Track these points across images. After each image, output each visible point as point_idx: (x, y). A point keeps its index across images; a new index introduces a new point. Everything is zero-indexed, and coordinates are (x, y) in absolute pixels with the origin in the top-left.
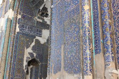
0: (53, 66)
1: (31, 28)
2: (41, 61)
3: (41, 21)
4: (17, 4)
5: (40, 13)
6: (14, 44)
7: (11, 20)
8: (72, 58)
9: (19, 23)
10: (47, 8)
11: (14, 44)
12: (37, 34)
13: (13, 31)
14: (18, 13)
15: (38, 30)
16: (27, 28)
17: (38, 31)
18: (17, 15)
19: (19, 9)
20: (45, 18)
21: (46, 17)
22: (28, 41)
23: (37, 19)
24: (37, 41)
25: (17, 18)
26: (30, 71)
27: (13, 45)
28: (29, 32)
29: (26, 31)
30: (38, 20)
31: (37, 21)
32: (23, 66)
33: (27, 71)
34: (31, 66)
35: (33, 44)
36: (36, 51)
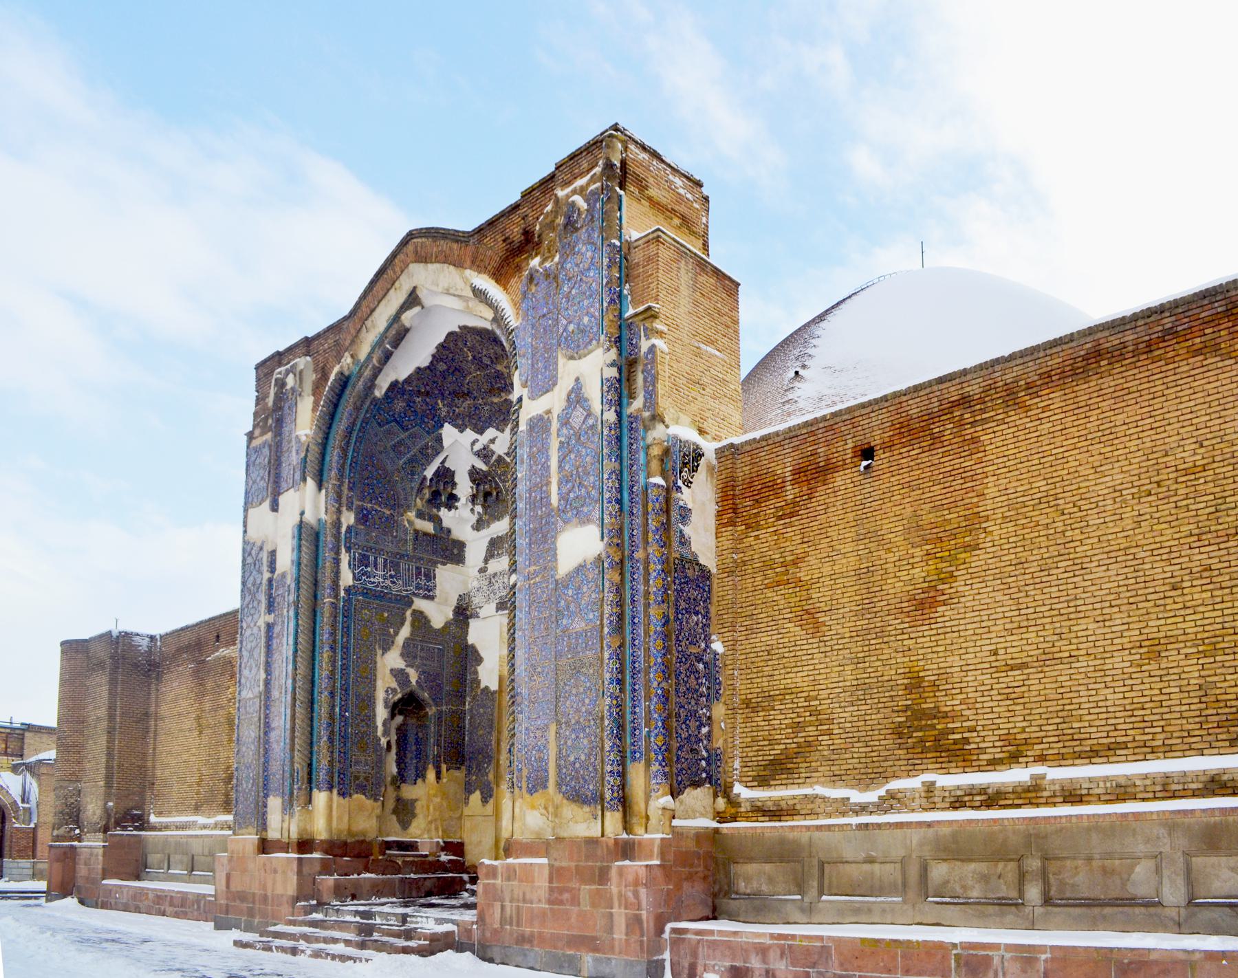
0: (525, 772)
1: (396, 566)
2: (437, 701)
5: (427, 494)
6: (339, 637)
7: (317, 535)
8: (577, 765)
9: (348, 550)
11: (339, 637)
12: (418, 587)
13: (328, 583)
16: (380, 566)
17: (420, 573)
18: (339, 512)
22: (387, 623)
24: (421, 620)
26: (394, 738)
27: (334, 641)
29: (378, 578)
31: (416, 532)
32: (375, 723)
33: (389, 743)
34: (399, 719)
35: (405, 632)
36: (418, 661)
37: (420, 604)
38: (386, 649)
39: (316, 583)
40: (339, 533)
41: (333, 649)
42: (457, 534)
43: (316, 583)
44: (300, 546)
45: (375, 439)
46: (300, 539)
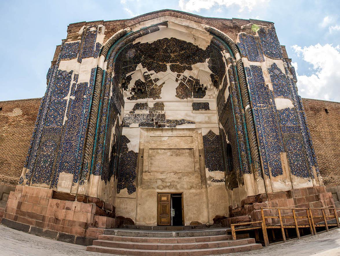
8: (299, 166)
38: (113, 126)
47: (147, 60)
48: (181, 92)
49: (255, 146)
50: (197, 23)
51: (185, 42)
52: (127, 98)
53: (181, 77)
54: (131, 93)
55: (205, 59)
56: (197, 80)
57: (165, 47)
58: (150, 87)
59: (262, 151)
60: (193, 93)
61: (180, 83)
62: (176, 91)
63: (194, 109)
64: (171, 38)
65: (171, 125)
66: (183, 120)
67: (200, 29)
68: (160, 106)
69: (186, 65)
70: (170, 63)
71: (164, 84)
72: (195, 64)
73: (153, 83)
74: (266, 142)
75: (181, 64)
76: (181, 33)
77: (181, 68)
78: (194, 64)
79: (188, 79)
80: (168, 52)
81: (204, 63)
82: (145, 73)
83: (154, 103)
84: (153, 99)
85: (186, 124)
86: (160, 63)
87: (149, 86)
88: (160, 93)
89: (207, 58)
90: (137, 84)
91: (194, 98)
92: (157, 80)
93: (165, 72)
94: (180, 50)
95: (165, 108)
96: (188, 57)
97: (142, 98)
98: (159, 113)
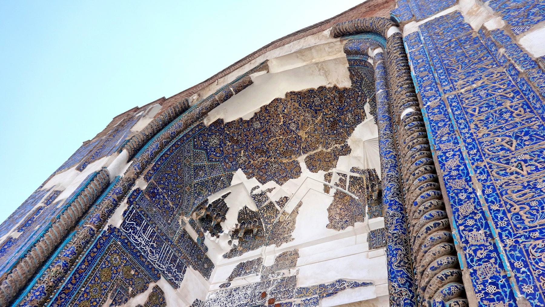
1: (160, 243)
3: (195, 236)
4: (152, 146)
5: (203, 213)
10: (228, 208)
11: (79, 261)
14: (145, 172)
15: (174, 260)
17: (175, 261)
18: (138, 175)
19: (152, 165)
20: (207, 234)
21: (213, 235)
22: (130, 280)
23: (186, 223)
25: (132, 184)
27: (73, 262)
28: (148, 249)
30: (187, 230)
31: (185, 232)
37: (163, 284)
39: (85, 213)
40: (129, 189)
41: (67, 268)
42: (210, 254)
43: (85, 213)
44: (89, 184)
45: (186, 154)
46: (92, 180)
47: (254, 160)
48: (340, 214)
49: (428, 229)
50: (316, 36)
51: (311, 91)
52: (224, 256)
53: (335, 179)
54: (230, 242)
55: (363, 108)
56: (369, 172)
57: (282, 120)
58: (272, 220)
59: (467, 242)
60: (367, 207)
61: (336, 194)
62: (327, 214)
63: (371, 247)
64: (287, 95)
65: (307, 302)
66: (339, 281)
67: (323, 42)
68: (289, 259)
69: (336, 145)
70: (304, 153)
71: (300, 206)
72: (352, 135)
73: (277, 210)
74: (489, 191)
75: (327, 149)
76: (295, 72)
77: (328, 158)
78: (349, 134)
79: (351, 177)
80: (292, 131)
81: (366, 121)
82: (254, 189)
83: (278, 255)
84: (274, 245)
85: (348, 290)
86: (285, 161)
87: (269, 218)
88: (291, 230)
89: (364, 104)
90: (242, 219)
91: (370, 218)
92: (284, 201)
93: (297, 177)
94: (313, 116)
95: (299, 261)
96: (334, 124)
97: (253, 249)
98: (284, 276)
